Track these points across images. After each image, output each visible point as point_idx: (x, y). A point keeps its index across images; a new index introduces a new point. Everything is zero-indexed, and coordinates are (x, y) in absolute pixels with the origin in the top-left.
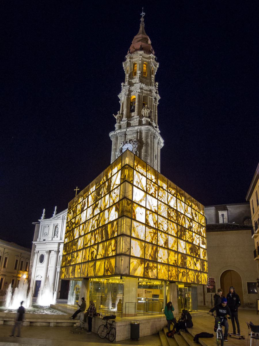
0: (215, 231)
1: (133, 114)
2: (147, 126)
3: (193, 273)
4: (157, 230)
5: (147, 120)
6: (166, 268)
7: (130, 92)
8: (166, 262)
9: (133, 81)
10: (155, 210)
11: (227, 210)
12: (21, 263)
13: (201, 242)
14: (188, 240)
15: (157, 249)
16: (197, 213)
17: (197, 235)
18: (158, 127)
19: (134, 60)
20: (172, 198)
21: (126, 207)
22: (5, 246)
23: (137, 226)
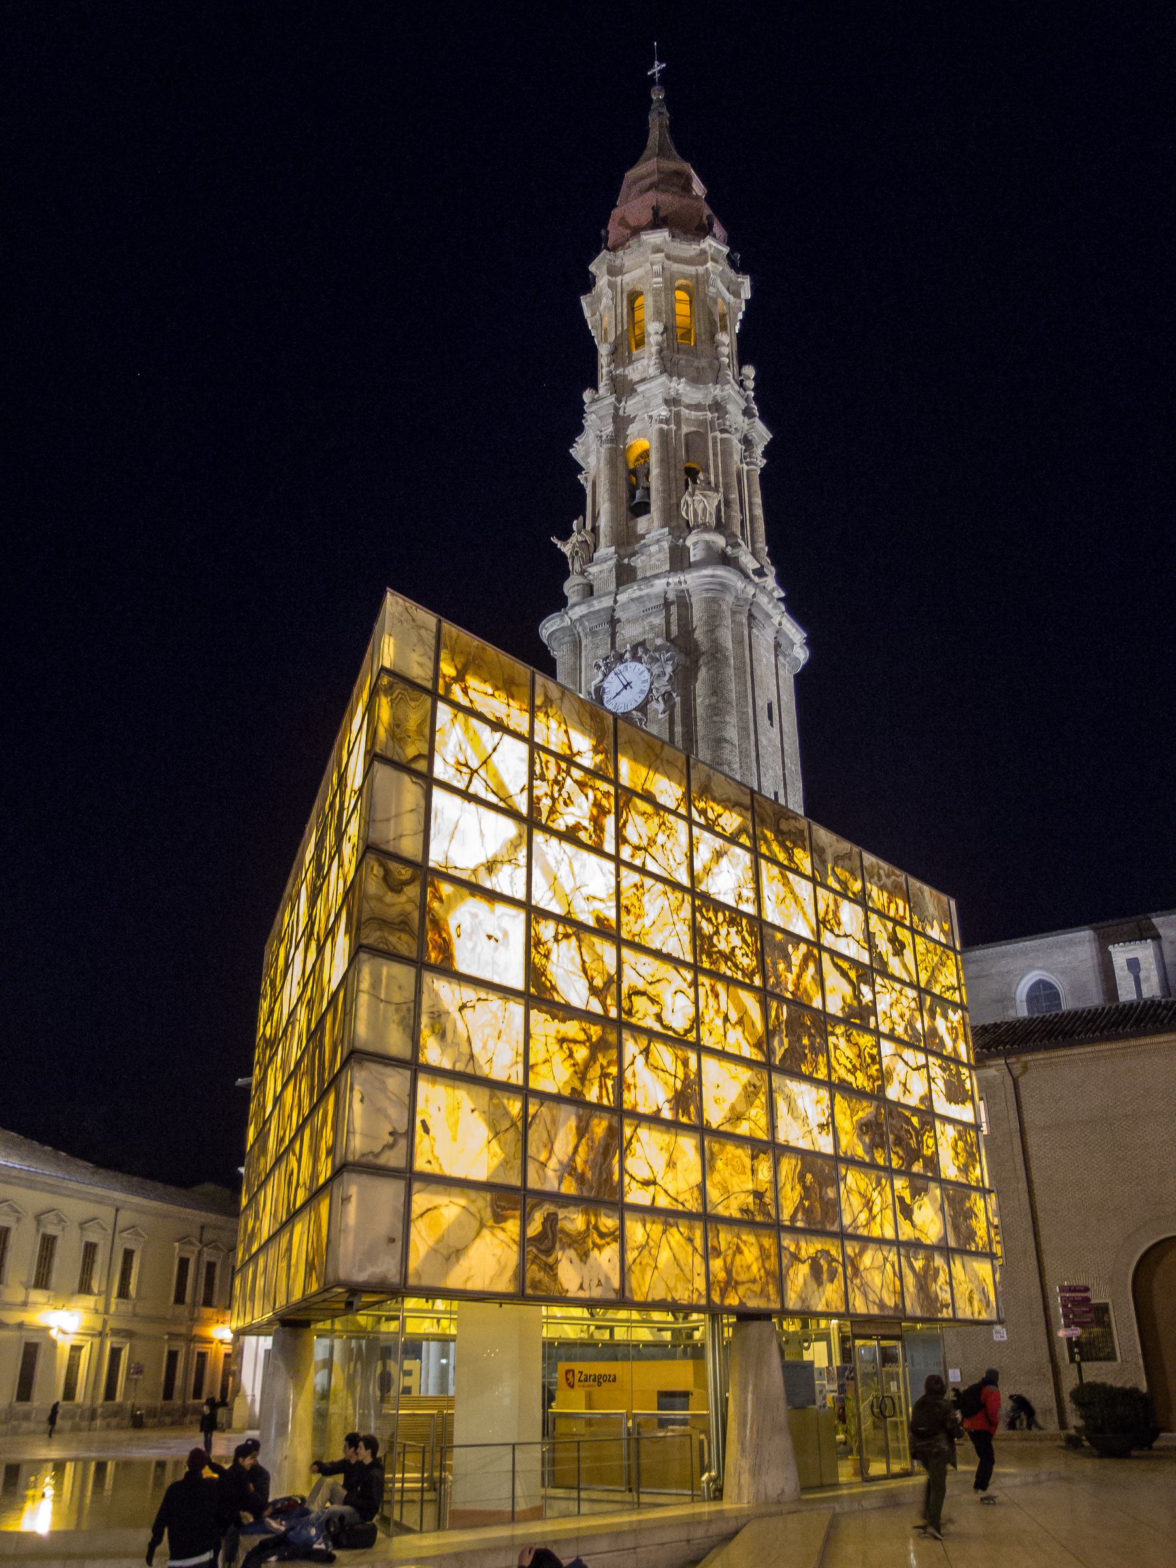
0: (1082, 1043)
1: (642, 524)
2: (708, 571)
3: (893, 1257)
4: (621, 1025)
5: (707, 542)
6: (690, 1240)
7: (621, 423)
8: (693, 1205)
9: (633, 373)
10: (598, 919)
11: (1157, 937)
12: (204, 1271)
13: (939, 1087)
14: (850, 1078)
15: (615, 1133)
16: (904, 935)
17: (908, 1054)
18: (771, 571)
19: (627, 278)
20: (719, 855)
21: (380, 899)
22: (118, 1196)
23: (462, 1008)
